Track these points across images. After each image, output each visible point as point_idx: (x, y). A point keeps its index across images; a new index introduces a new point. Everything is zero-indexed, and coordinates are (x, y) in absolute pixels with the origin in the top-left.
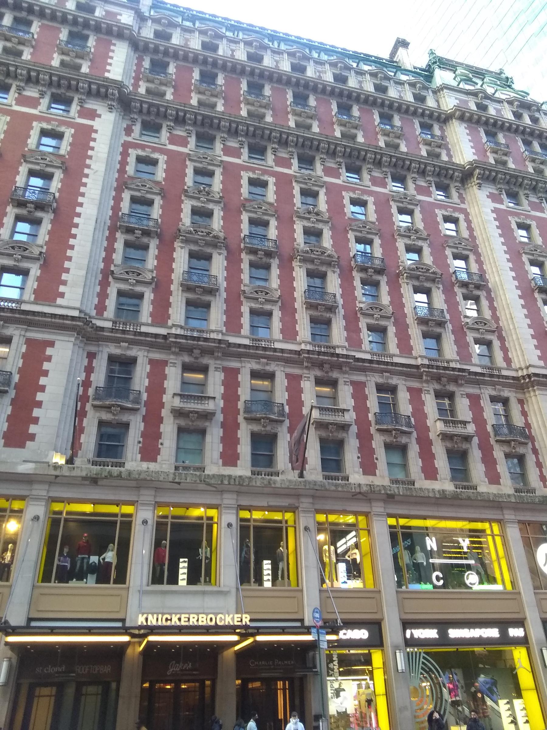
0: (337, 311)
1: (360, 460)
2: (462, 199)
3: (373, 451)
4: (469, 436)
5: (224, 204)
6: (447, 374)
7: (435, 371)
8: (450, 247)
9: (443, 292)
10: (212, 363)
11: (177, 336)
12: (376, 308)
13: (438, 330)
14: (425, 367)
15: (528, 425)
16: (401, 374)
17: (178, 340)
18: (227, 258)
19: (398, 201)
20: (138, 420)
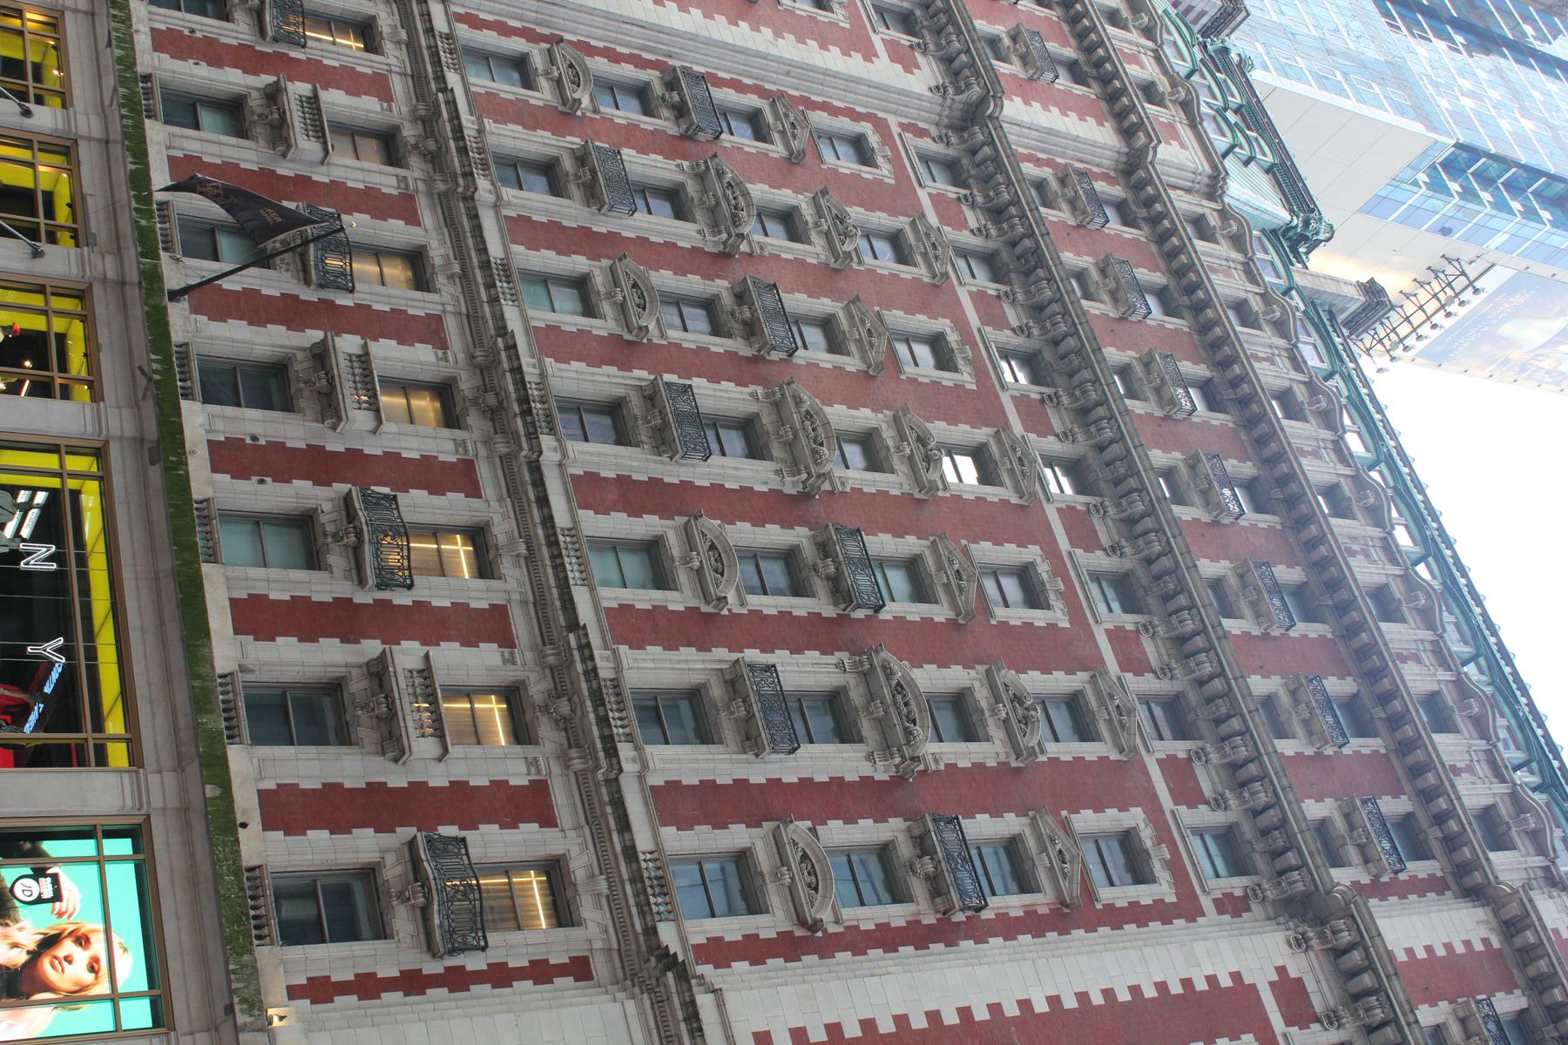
0: (665, 458)
1: (248, 441)
2: (1232, 906)
3: (284, 477)
4: (399, 739)
5: (836, 271)
6: (584, 713)
7: (579, 667)
8: (1034, 824)
9: (866, 781)
10: (416, 170)
11: (452, 103)
12: (719, 559)
13: (728, 732)
14: (578, 638)
15: (500, 976)
16: (538, 589)
17: (443, 107)
18: (695, 250)
19: (1098, 693)
20: (284, 285)
